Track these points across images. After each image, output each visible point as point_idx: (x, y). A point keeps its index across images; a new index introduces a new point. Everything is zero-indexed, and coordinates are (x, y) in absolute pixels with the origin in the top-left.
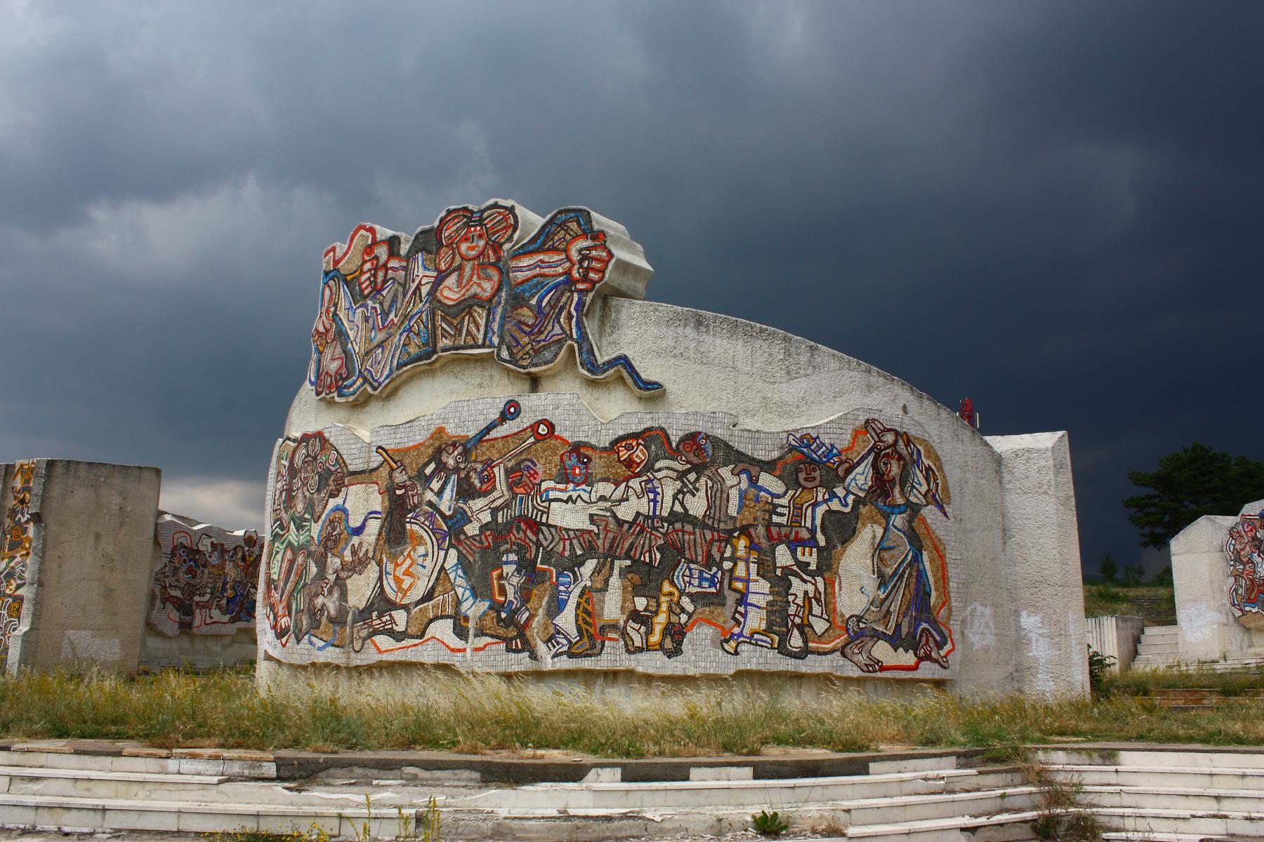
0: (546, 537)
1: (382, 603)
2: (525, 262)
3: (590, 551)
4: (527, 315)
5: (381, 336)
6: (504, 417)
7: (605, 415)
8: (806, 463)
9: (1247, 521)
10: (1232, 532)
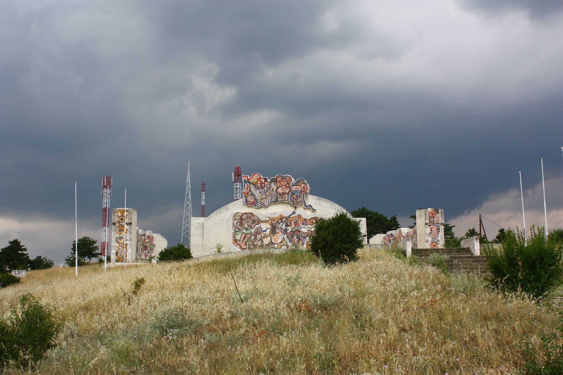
0: (301, 233)
1: (271, 243)
2: (294, 187)
3: (308, 236)
4: (295, 197)
5: (265, 197)
6: (293, 214)
9: (388, 235)
10: (384, 238)
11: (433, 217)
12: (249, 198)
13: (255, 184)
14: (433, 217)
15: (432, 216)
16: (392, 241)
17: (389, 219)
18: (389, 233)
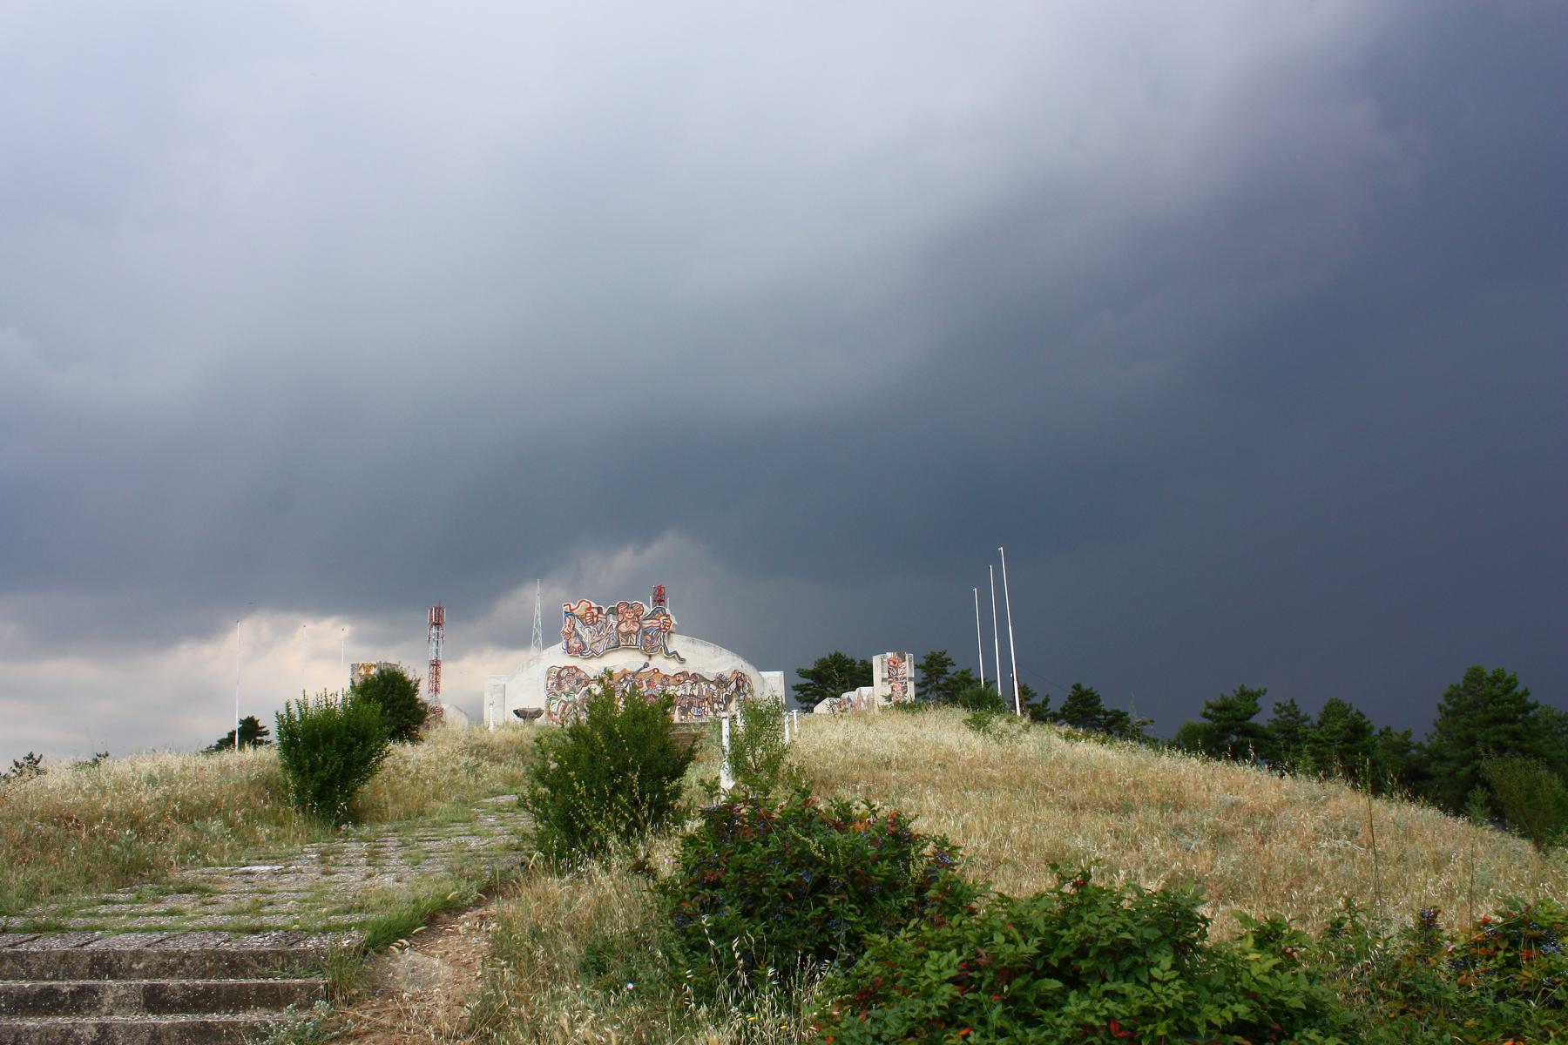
7: (671, 667)
8: (721, 682)
12: (572, 642)
13: (581, 618)
18: (845, 695)
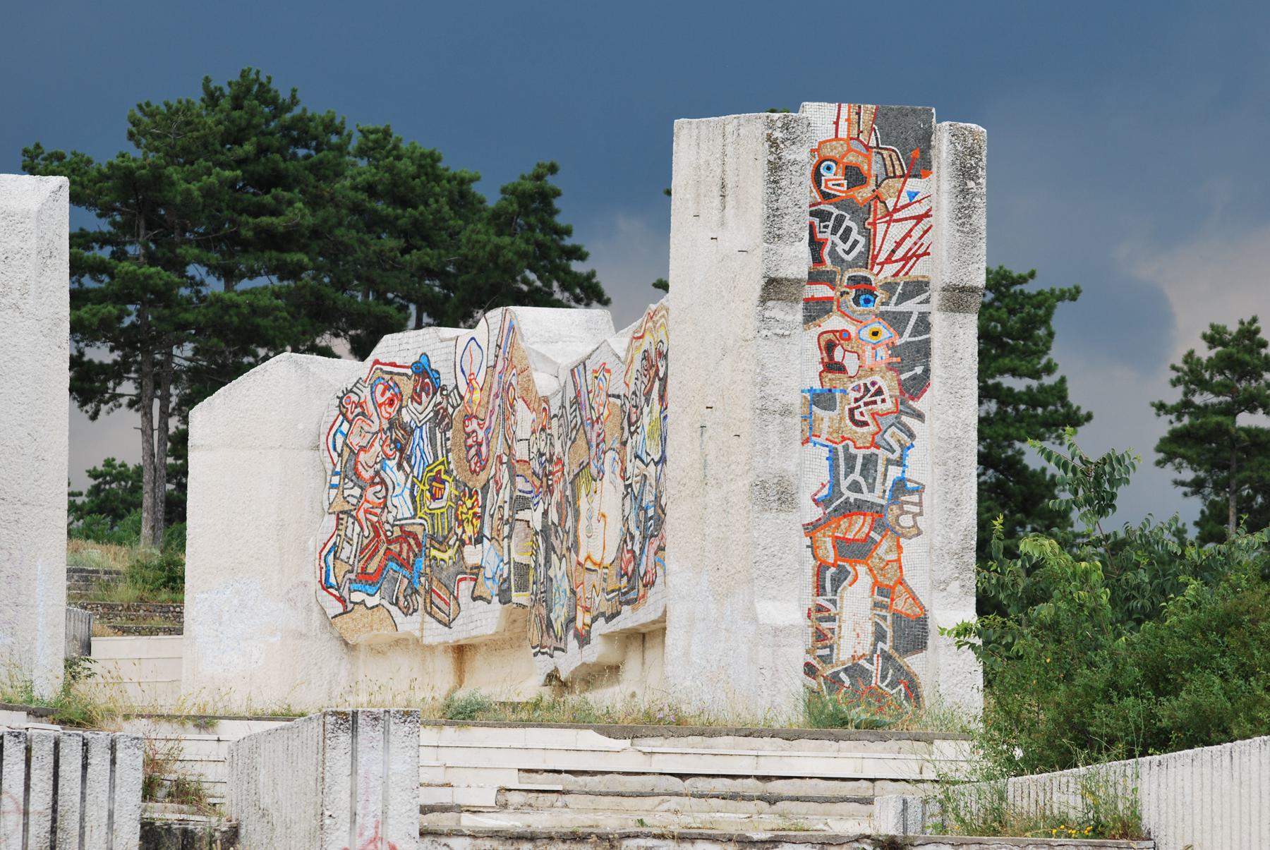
9: (386, 379)
10: (348, 407)
11: (862, 213)
14: (862, 213)
15: (841, 206)
16: (421, 445)
17: (490, 194)
18: (397, 348)
